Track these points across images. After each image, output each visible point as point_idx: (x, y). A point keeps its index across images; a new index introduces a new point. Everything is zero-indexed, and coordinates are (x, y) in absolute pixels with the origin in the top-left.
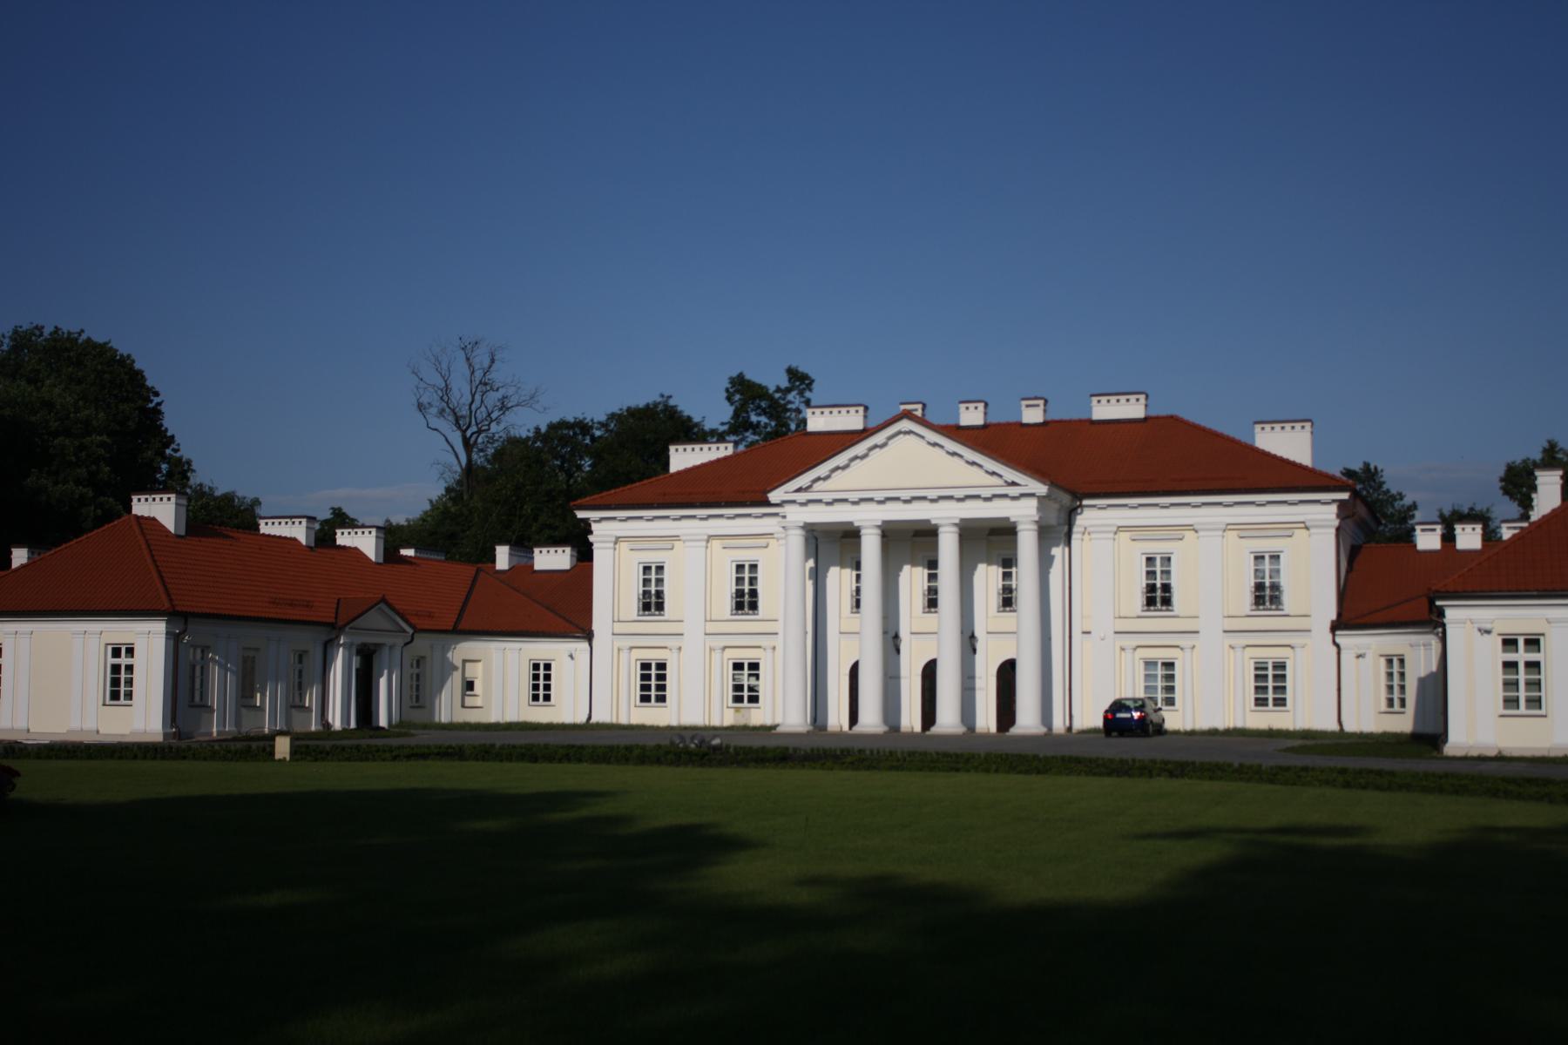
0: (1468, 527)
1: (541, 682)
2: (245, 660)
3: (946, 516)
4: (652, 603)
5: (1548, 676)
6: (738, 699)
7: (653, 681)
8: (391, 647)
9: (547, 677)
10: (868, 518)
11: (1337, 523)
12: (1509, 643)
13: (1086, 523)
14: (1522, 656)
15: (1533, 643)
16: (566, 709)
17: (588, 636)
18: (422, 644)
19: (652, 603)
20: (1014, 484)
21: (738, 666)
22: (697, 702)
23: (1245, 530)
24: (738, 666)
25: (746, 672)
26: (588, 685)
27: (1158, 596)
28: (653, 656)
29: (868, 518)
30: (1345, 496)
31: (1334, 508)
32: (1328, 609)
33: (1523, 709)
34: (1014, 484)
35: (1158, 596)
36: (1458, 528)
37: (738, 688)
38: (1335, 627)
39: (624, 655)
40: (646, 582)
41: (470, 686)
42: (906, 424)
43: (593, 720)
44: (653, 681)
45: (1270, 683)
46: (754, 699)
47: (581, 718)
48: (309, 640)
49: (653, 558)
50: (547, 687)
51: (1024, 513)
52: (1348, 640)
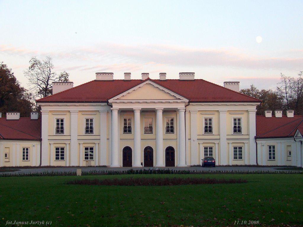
0: (279, 112)
4: (60, 130)
6: (86, 158)
7: (60, 154)
9: (27, 152)
10: (137, 108)
11: (256, 110)
13: (189, 109)
16: (34, 161)
17: (40, 140)
19: (60, 130)
21: (87, 149)
22: (75, 158)
23: (230, 112)
24: (87, 149)
25: (89, 150)
26: (41, 155)
27: (208, 129)
29: (137, 108)
30: (259, 104)
31: (255, 107)
32: (253, 133)
33: (238, 159)
35: (208, 129)
36: (276, 112)
37: (86, 155)
38: (256, 138)
39: (81, 146)
41: (6, 155)
43: (42, 165)
44: (60, 154)
45: (238, 152)
46: (92, 158)
47: (38, 165)
51: (181, 106)
52: (259, 142)
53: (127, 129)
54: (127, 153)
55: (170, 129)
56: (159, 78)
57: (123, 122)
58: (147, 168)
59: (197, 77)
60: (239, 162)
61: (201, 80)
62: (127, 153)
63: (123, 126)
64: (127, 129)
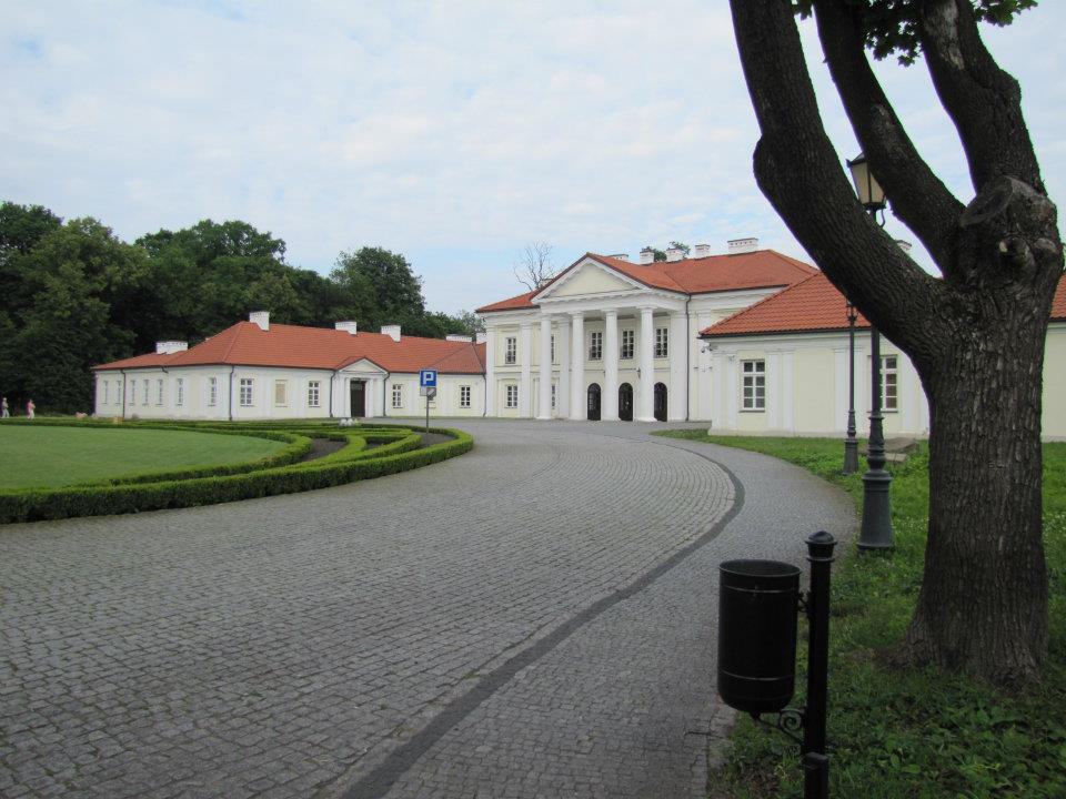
1: (466, 395)
2: (278, 386)
3: (610, 309)
4: (511, 358)
5: (768, 386)
7: (512, 399)
8: (375, 380)
12: (748, 366)
14: (754, 374)
15: (761, 366)
17: (484, 374)
18: (395, 379)
19: (511, 358)
20: (637, 288)
28: (512, 383)
34: (637, 288)
40: (510, 347)
42: (588, 260)
44: (512, 399)
48: (323, 378)
49: (511, 335)
50: (468, 399)
53: (596, 353)
54: (595, 394)
55: (661, 351)
56: (728, 252)
57: (590, 338)
58: (356, 422)
59: (761, 247)
60: (465, 412)
61: (768, 251)
62: (595, 394)
63: (622, 344)
64: (596, 353)
